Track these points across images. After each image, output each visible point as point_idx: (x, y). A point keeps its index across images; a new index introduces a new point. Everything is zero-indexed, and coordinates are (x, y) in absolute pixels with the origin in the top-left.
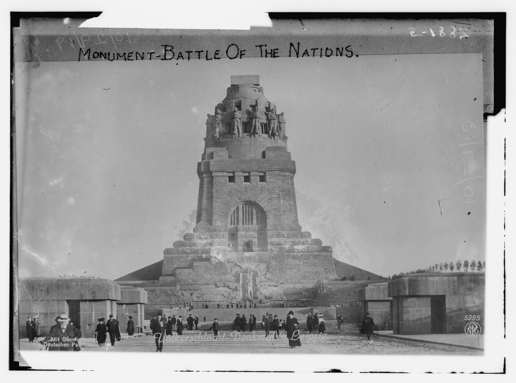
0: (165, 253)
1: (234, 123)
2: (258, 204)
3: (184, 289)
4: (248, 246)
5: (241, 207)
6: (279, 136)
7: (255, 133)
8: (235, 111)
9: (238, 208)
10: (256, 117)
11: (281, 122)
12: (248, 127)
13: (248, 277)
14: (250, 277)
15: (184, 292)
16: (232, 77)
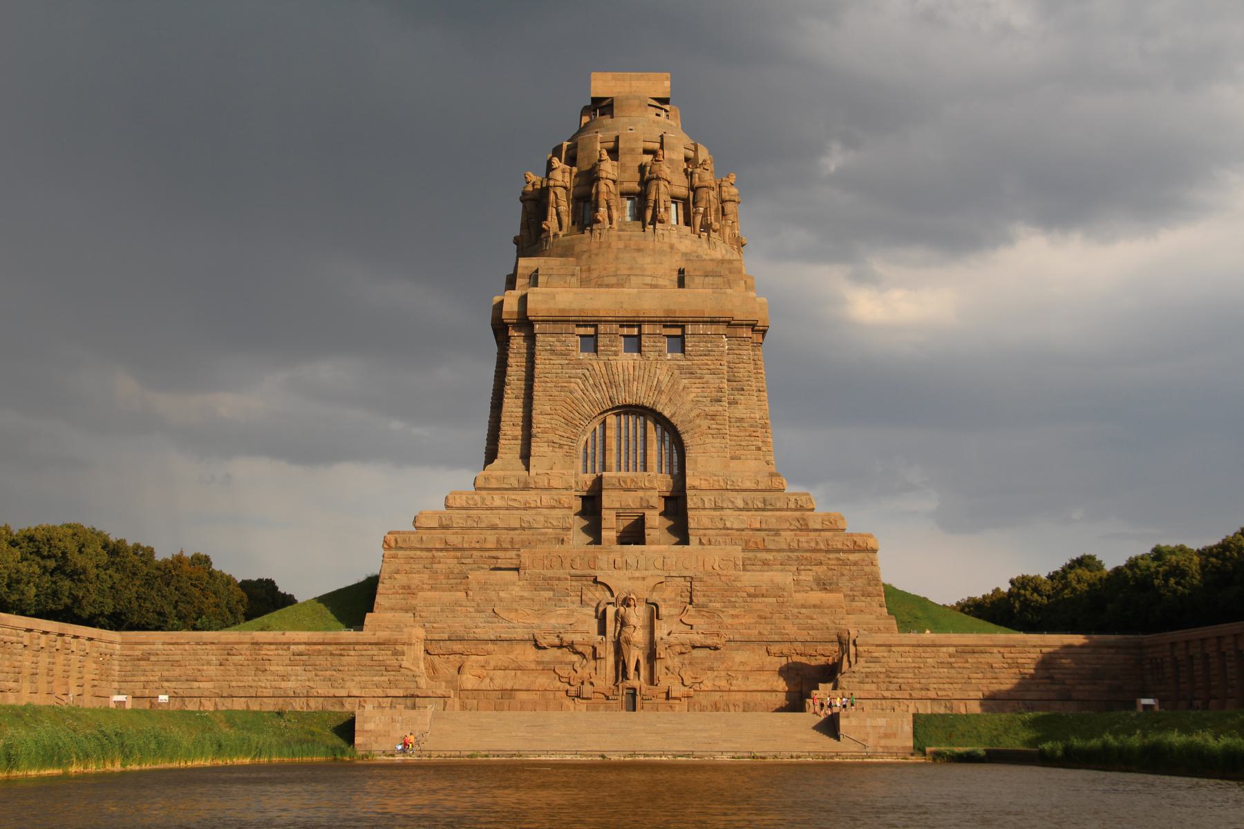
1: (598, 193)
2: (660, 414)
4: (634, 534)
6: (722, 235)
7: (655, 219)
8: (600, 161)
9: (604, 422)
10: (658, 178)
14: (637, 615)
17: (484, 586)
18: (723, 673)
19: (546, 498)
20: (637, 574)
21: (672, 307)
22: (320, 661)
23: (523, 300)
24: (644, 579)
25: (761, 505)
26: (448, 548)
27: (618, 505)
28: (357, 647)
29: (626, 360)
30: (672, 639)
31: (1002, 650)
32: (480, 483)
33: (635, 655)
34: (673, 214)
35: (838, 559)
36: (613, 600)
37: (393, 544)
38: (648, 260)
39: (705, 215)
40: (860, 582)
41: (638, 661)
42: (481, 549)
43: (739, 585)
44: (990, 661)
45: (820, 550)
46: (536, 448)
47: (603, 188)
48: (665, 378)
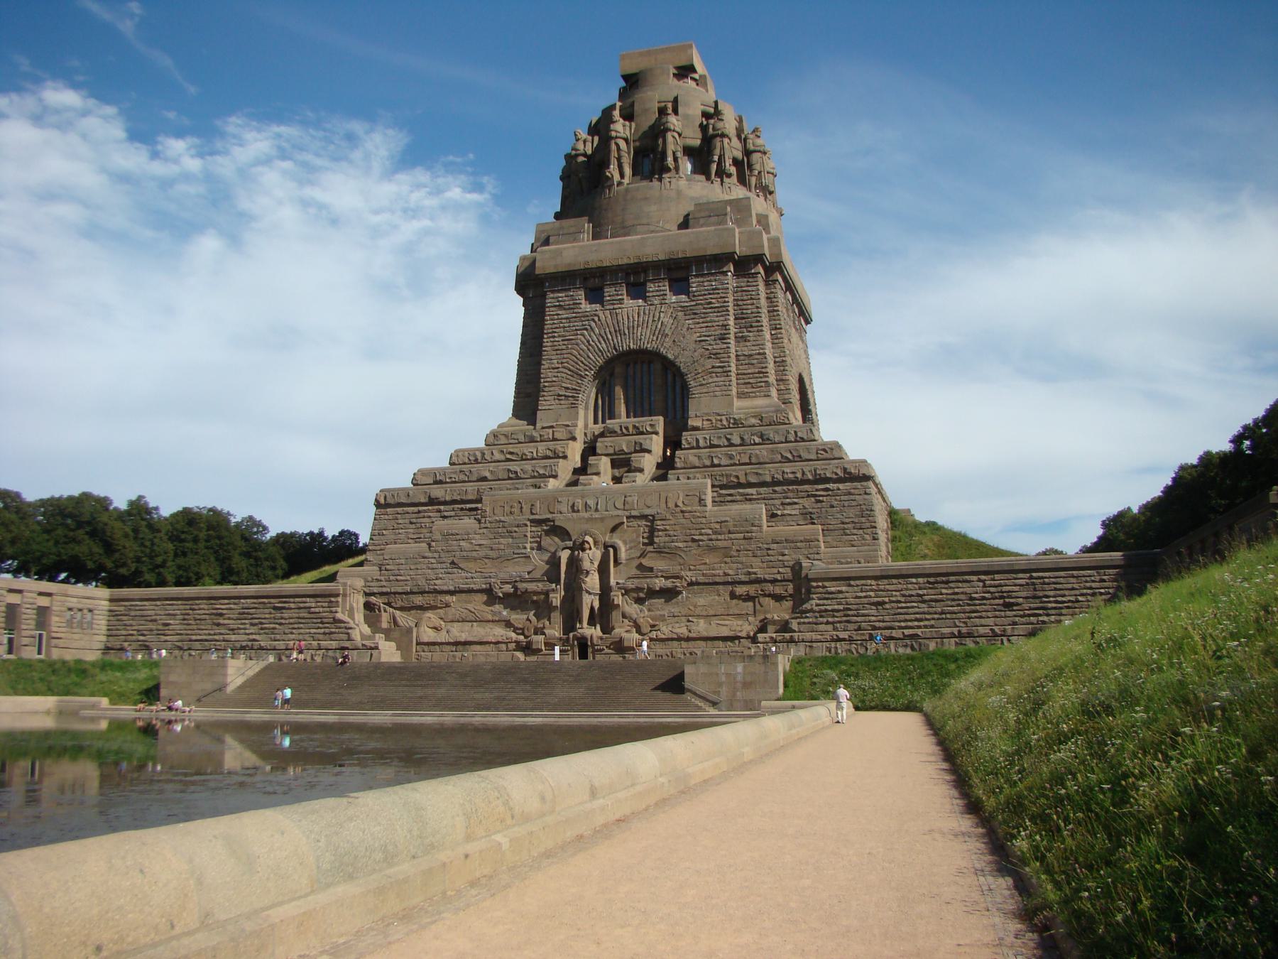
0: (378, 505)
3: (400, 604)
10: (668, 130)
11: (751, 147)
12: (650, 159)
13: (586, 565)
14: (591, 558)
15: (398, 613)
16: (623, 57)
17: (447, 536)
18: (684, 619)
19: (542, 448)
20: (597, 515)
24: (602, 519)
25: (757, 440)
26: (432, 502)
27: (611, 451)
29: (631, 305)
30: (630, 585)
31: (983, 577)
32: (491, 440)
33: (590, 601)
34: (687, 166)
35: (827, 490)
36: (570, 544)
37: (382, 501)
38: (654, 208)
39: (719, 164)
40: (852, 513)
41: (592, 608)
42: (463, 502)
43: (704, 520)
44: (968, 590)
45: (808, 482)
46: (543, 404)
47: (613, 147)
48: (667, 320)
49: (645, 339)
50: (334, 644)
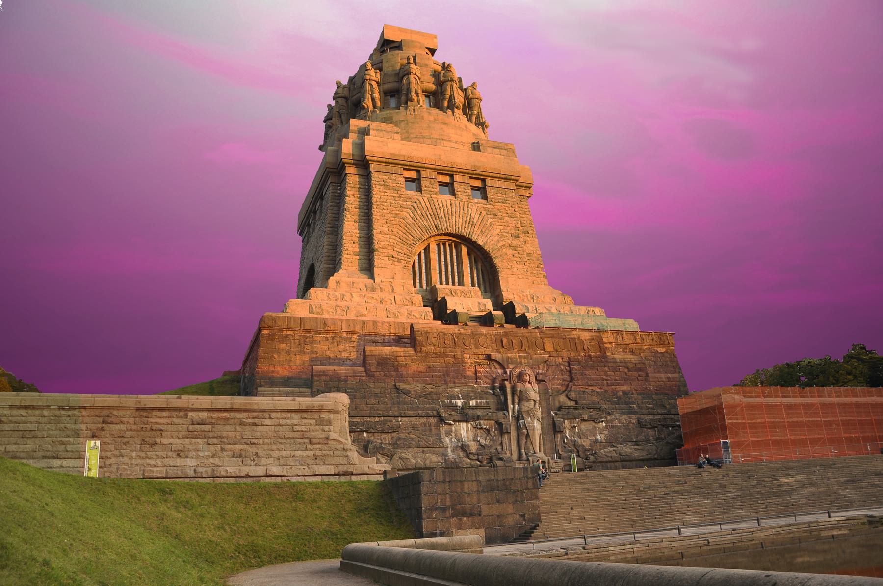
2: (475, 242)
5: (433, 247)
9: (427, 250)
21: (477, 164)
22: (228, 431)
23: (361, 146)
28: (273, 415)
29: (445, 198)
49: (458, 225)
50: (331, 470)
